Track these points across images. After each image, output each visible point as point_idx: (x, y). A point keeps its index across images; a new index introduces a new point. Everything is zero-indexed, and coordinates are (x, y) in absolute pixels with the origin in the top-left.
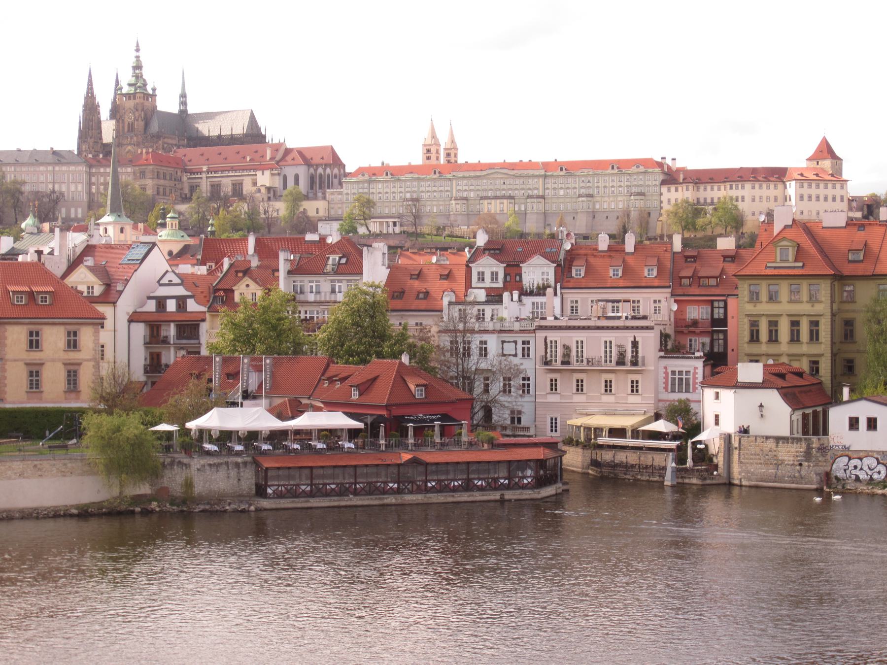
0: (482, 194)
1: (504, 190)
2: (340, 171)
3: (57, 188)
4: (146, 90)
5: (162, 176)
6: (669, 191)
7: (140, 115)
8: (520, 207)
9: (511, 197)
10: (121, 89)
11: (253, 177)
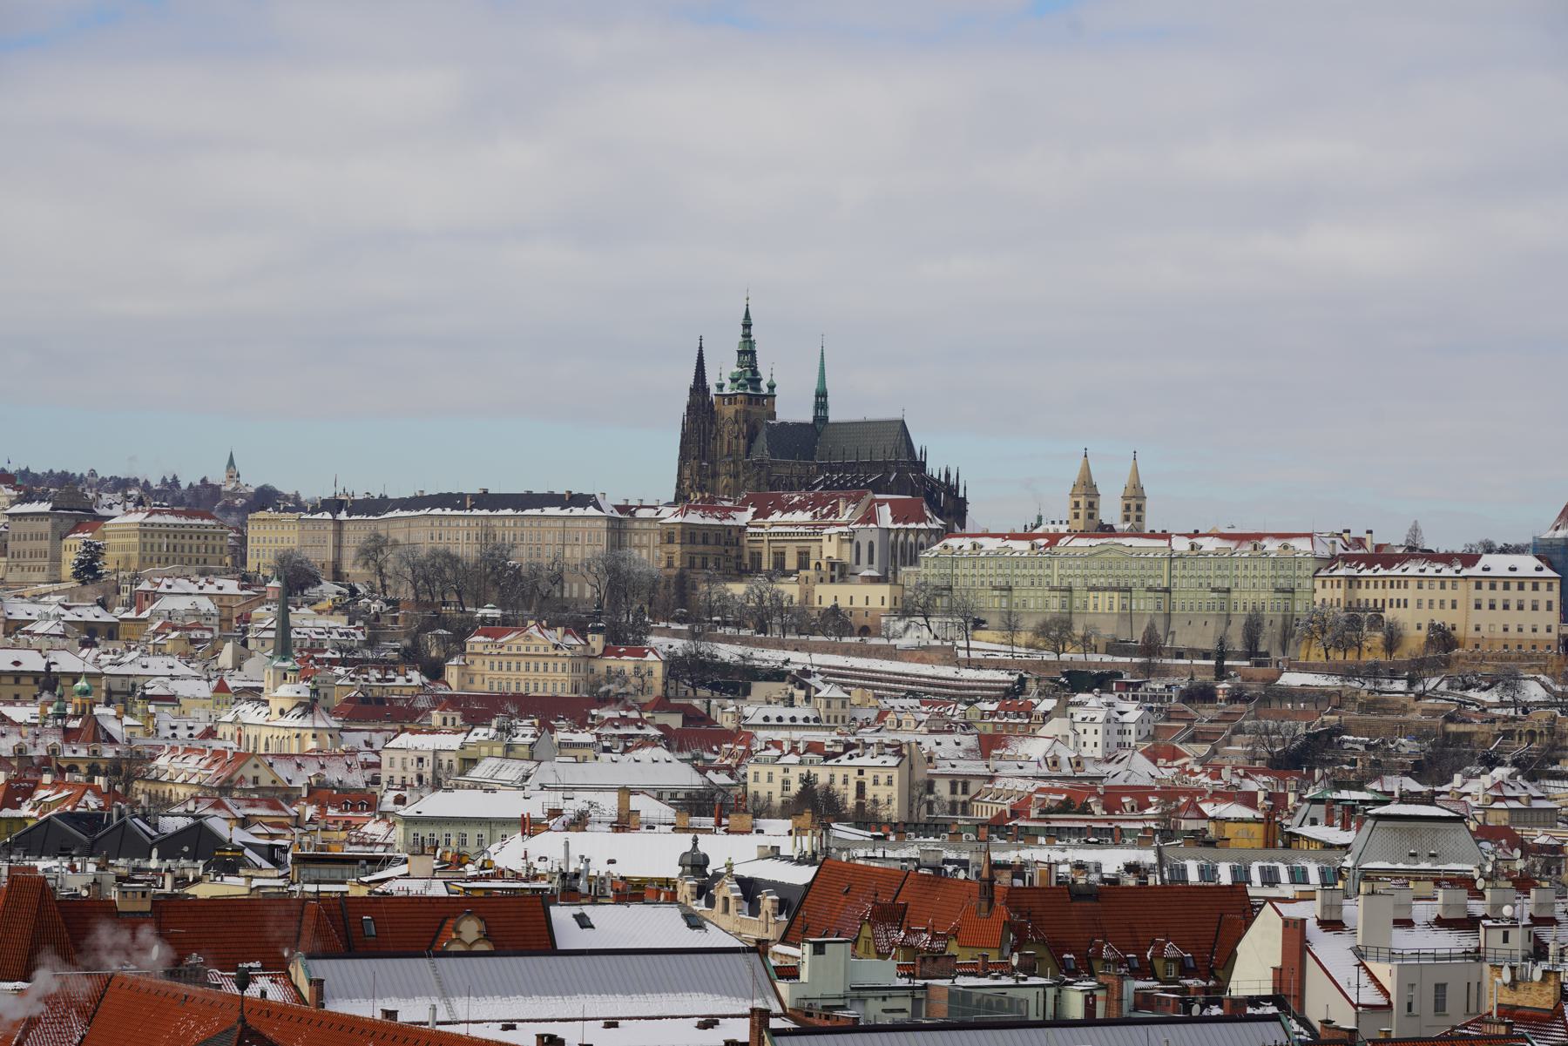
4: (759, 390)
5: (699, 539)
6: (1324, 586)
7: (740, 429)
8: (1138, 605)
10: (720, 387)
11: (818, 544)
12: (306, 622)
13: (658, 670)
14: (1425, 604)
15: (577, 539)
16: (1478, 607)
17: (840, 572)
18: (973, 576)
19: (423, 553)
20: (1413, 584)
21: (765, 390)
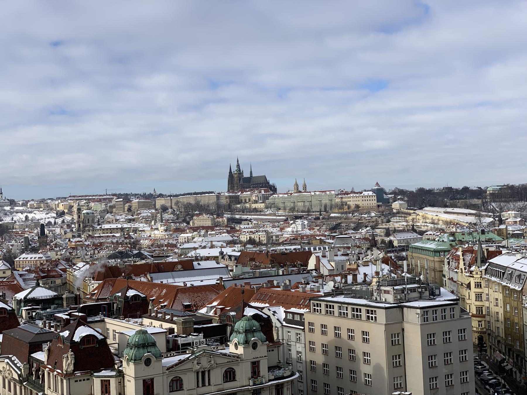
10: (234, 172)
12: (166, 216)
13: (226, 220)
14: (354, 201)
16: (363, 201)
17: (256, 202)
19: (185, 203)
20: (352, 198)
21: (242, 172)
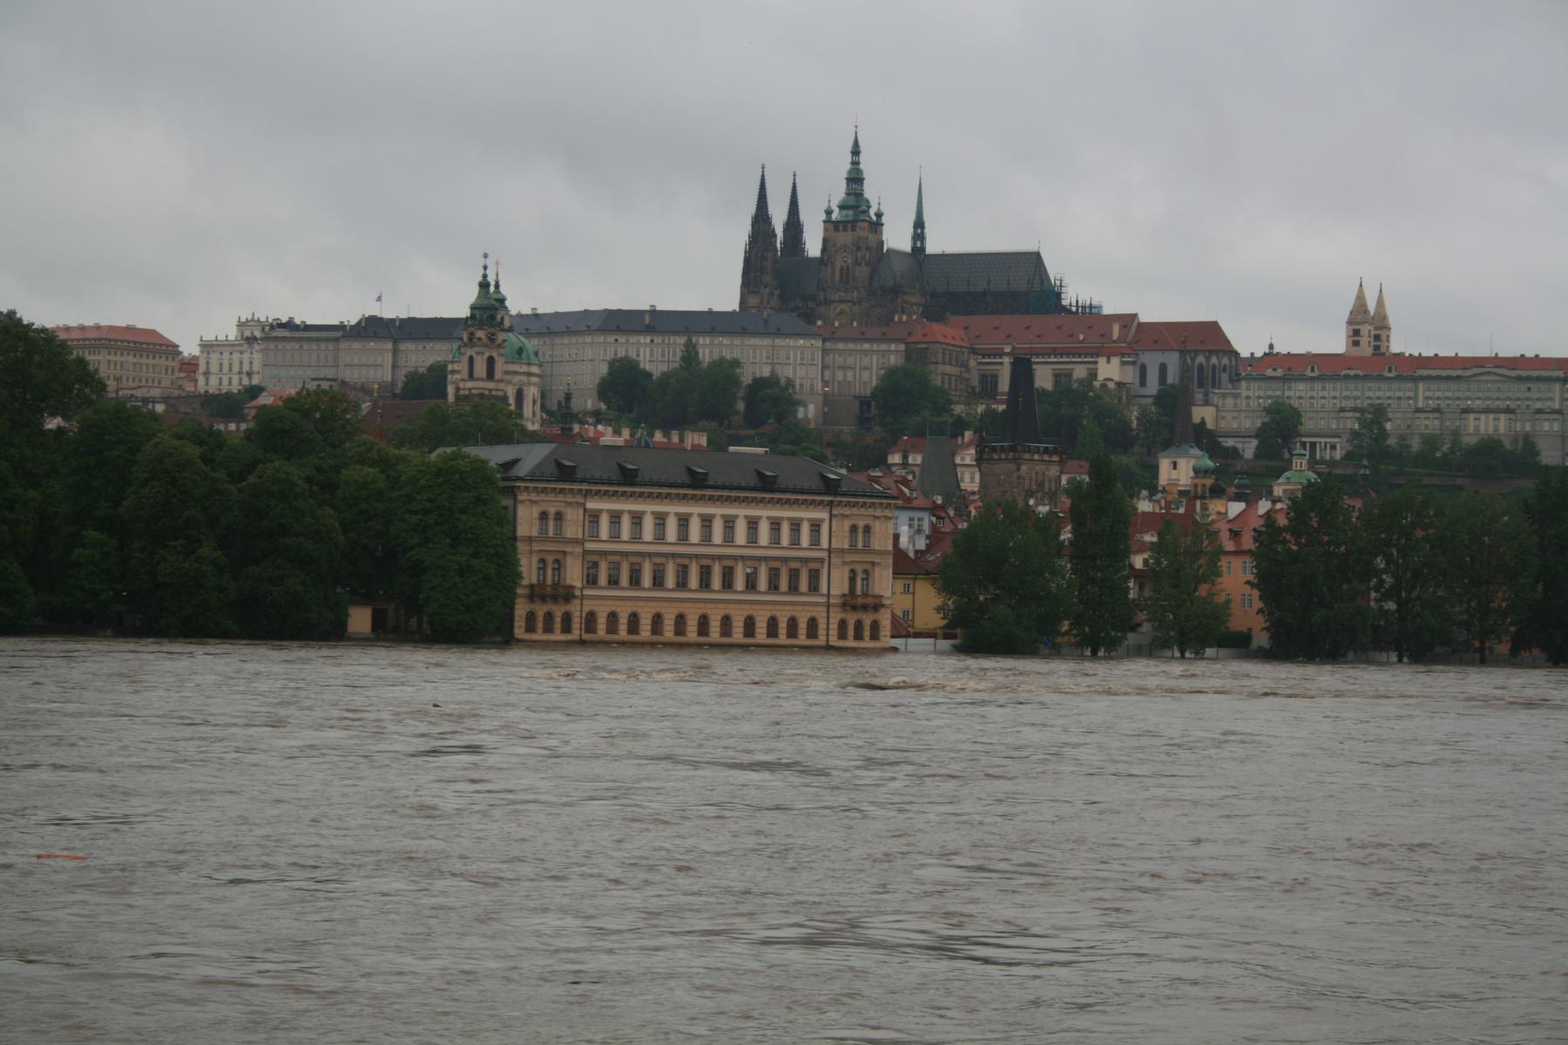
0: (1463, 404)
1: (1498, 399)
2: (1231, 362)
3: (778, 370)
4: (870, 217)
9: (1508, 411)
11: (1092, 366)
15: (788, 358)
18: (1312, 398)
21: (874, 218)
